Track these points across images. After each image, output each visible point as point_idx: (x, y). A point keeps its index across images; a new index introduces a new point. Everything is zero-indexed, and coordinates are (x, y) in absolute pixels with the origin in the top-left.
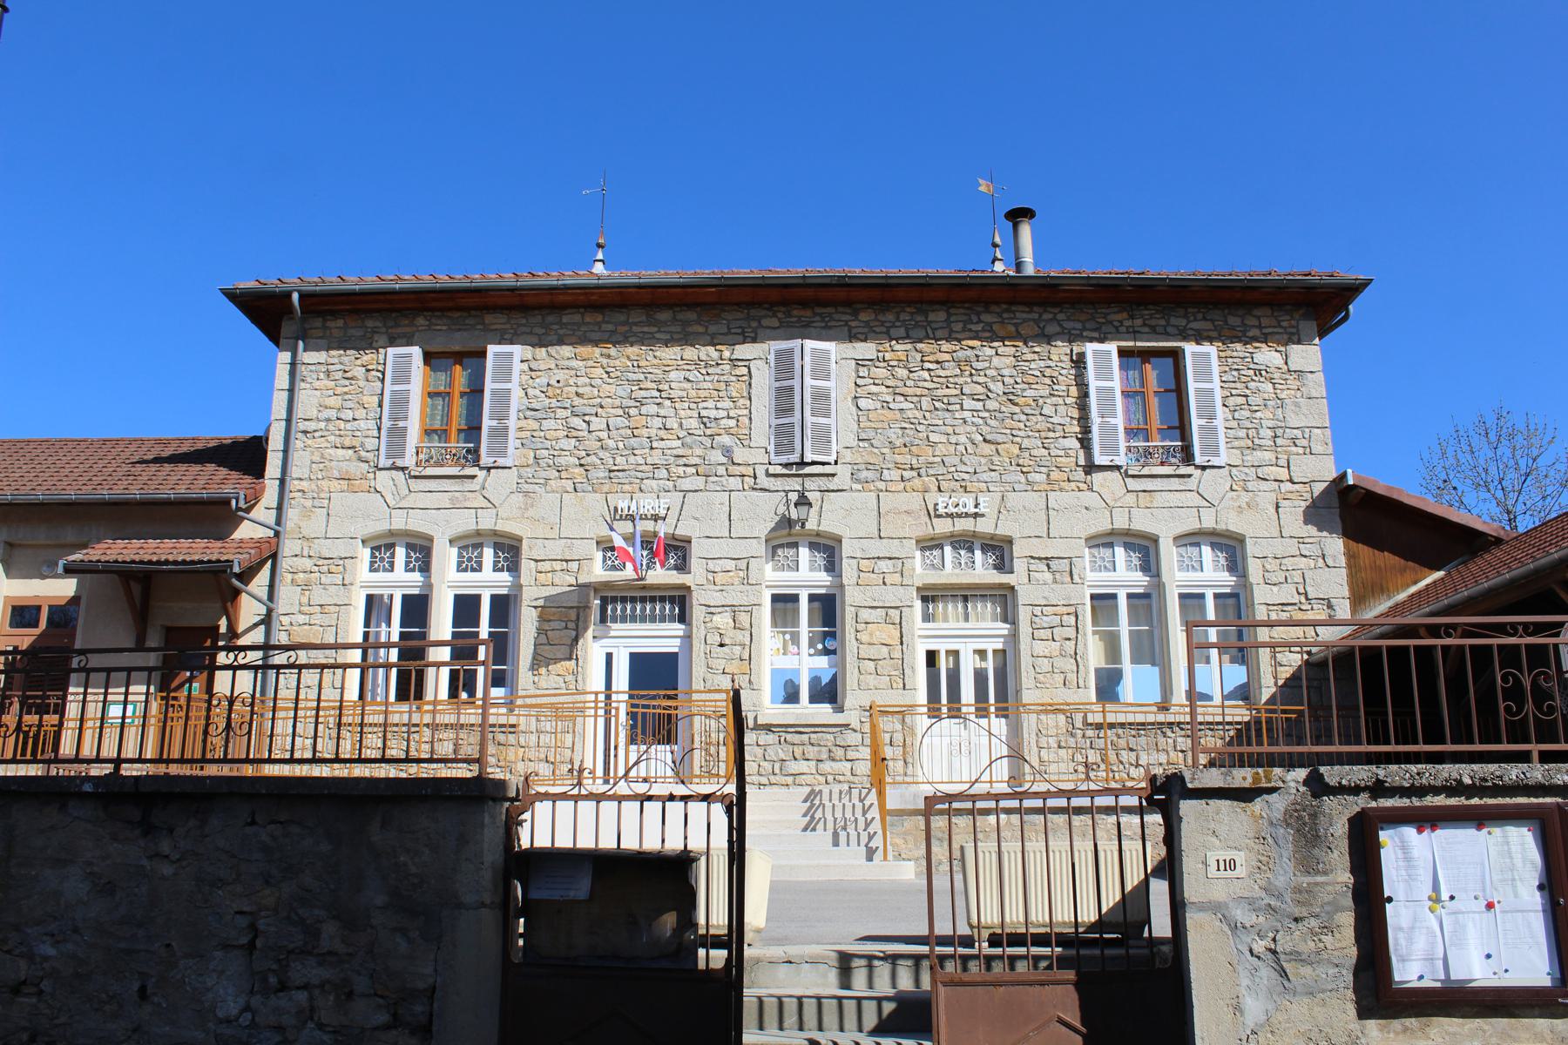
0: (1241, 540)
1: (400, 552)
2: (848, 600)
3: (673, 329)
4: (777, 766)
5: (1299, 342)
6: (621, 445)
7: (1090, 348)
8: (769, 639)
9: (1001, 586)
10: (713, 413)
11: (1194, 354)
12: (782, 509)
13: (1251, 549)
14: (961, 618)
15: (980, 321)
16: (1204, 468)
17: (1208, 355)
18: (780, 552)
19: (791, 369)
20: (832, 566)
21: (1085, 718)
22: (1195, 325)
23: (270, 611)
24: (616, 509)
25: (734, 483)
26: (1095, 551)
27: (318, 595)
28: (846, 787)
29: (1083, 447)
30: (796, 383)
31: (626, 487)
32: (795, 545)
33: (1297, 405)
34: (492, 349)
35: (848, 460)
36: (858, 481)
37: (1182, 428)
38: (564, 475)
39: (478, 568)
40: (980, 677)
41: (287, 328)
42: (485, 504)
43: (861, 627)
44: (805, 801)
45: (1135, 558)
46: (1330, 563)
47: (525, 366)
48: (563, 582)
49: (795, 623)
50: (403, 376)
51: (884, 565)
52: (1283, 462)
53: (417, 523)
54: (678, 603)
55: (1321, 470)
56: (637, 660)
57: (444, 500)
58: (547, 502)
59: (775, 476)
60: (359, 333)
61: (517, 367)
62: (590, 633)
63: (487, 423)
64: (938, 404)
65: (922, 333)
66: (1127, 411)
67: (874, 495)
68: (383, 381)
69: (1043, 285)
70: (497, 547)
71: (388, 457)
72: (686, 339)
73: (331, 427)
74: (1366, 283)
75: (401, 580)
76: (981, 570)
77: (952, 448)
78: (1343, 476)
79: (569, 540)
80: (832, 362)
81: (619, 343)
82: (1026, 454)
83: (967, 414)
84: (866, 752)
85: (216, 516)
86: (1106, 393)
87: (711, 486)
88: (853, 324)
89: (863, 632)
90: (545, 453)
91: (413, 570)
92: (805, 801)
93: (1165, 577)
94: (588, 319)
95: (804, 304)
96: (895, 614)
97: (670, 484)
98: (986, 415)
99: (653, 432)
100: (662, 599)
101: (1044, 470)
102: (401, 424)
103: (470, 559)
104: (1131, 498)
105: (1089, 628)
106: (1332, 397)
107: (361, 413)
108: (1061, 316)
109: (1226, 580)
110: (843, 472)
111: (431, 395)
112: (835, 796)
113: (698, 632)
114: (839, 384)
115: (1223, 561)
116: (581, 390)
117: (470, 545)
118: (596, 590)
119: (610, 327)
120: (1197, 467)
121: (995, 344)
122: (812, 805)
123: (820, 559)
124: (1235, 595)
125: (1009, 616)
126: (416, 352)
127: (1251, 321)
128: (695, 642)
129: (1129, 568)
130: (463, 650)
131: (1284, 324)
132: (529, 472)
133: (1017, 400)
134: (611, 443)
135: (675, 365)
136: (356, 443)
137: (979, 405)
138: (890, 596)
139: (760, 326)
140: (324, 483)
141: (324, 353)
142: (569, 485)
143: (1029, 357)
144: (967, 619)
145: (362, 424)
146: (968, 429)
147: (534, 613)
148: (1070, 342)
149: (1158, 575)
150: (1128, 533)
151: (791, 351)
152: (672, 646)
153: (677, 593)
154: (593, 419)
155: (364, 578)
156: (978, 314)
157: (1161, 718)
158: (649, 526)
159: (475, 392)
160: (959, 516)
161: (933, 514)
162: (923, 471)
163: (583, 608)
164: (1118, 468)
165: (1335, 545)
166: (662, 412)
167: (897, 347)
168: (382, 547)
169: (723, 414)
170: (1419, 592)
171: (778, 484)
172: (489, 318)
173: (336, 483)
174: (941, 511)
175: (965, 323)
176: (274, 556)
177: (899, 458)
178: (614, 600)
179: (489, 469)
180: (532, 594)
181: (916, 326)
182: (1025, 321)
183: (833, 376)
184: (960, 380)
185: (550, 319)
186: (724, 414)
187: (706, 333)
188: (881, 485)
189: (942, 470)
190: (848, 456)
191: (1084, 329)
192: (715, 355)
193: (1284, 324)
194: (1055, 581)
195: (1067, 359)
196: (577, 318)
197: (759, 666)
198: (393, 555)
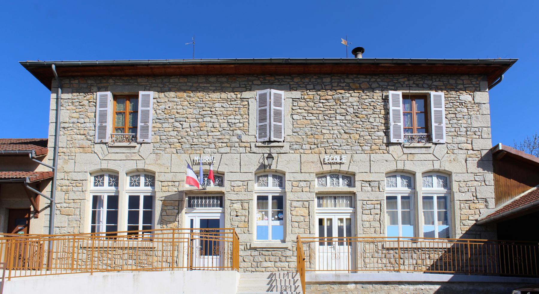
0: (449, 174)
1: (106, 178)
2: (288, 198)
3: (217, 85)
5: (480, 91)
6: (195, 134)
7: (391, 93)
8: (256, 213)
9: (350, 193)
10: (233, 121)
11: (434, 96)
12: (261, 161)
13: (454, 177)
14: (333, 205)
15: (344, 82)
16: (436, 144)
17: (440, 96)
18: (261, 179)
19: (265, 102)
20: (281, 184)
21: (383, 245)
22: (435, 83)
23: (51, 203)
24: (194, 160)
25: (242, 150)
26: (389, 179)
27: (72, 196)
28: (286, 272)
29: (386, 135)
30: (267, 108)
31: (198, 152)
32: (267, 176)
33: (477, 118)
34: (141, 93)
36: (292, 149)
37: (427, 127)
38: (172, 146)
39: (138, 185)
40: (340, 229)
41: (54, 83)
43: (293, 209)
44: (268, 278)
45: (405, 182)
46: (487, 183)
47: (155, 101)
48: (173, 190)
49: (267, 207)
50: (104, 104)
51: (302, 184)
52: (469, 142)
53: (112, 166)
54: (219, 199)
55: (486, 145)
56: (202, 221)
57: (123, 157)
58: (165, 157)
60: (85, 86)
61: (152, 101)
62: (184, 211)
63: (140, 124)
64: (326, 117)
65: (320, 87)
66: (404, 121)
67: (299, 155)
68: (96, 106)
69: (373, 64)
70: (146, 176)
71: (99, 138)
72: (222, 90)
73: (75, 126)
75: (106, 190)
76: (342, 186)
78: (498, 146)
79: (176, 173)
80: (284, 100)
81: (194, 91)
83: (338, 122)
84: (295, 259)
85: (25, 162)
86: (396, 112)
88: (291, 83)
90: (164, 137)
91: (112, 186)
92: (268, 278)
93: (418, 189)
94: (181, 81)
95: (271, 74)
96: (306, 204)
98: (346, 122)
99: (209, 129)
100: (213, 198)
101: (369, 145)
102: (104, 124)
103: (135, 181)
104: (405, 157)
105: (386, 210)
106: (492, 114)
107: (87, 120)
108: (378, 80)
109: (442, 191)
110: (286, 145)
111: (118, 113)
112: (282, 276)
113: (228, 211)
114: (285, 108)
115: (441, 183)
116: (178, 111)
117: (135, 175)
118: (186, 194)
119: (190, 84)
120: (433, 143)
121: (351, 92)
122: (271, 280)
123: (277, 182)
124: (445, 198)
126: (109, 94)
127: (460, 82)
128: (226, 215)
129: (402, 186)
130: (133, 217)
131: (474, 83)
132: (157, 145)
133: (359, 115)
134: (191, 133)
135: (218, 101)
136: (86, 132)
137: (343, 118)
138: (305, 196)
139: (253, 84)
140: (73, 149)
141: (70, 94)
143: (365, 97)
144: (335, 206)
145: (88, 125)
146: (338, 128)
147: (161, 203)
148: (382, 91)
149: (414, 188)
150: (403, 171)
151: (266, 94)
152: (217, 216)
154: (184, 123)
155: (91, 188)
156: (344, 79)
157: (414, 245)
158: (207, 167)
159: (135, 112)
160: (334, 164)
161: (323, 163)
162: (319, 145)
163: (181, 201)
164: (400, 144)
165: (490, 176)
166: (212, 120)
167: (310, 93)
168: (99, 176)
169: (238, 121)
170: (525, 196)
172: (140, 80)
173: (78, 149)
174: (326, 161)
175: (338, 83)
176: (52, 179)
177: (309, 140)
178: (194, 198)
179: (141, 144)
181: (317, 84)
182: (363, 82)
183: (283, 105)
184: (336, 107)
185: (165, 80)
186: (238, 121)
187: (230, 87)
188: (302, 151)
189: (327, 145)
190: (288, 139)
191: (388, 85)
192: (234, 96)
193: (474, 83)
194: (372, 191)
195: (380, 98)
196: (176, 80)
197: (252, 224)
198: (103, 179)
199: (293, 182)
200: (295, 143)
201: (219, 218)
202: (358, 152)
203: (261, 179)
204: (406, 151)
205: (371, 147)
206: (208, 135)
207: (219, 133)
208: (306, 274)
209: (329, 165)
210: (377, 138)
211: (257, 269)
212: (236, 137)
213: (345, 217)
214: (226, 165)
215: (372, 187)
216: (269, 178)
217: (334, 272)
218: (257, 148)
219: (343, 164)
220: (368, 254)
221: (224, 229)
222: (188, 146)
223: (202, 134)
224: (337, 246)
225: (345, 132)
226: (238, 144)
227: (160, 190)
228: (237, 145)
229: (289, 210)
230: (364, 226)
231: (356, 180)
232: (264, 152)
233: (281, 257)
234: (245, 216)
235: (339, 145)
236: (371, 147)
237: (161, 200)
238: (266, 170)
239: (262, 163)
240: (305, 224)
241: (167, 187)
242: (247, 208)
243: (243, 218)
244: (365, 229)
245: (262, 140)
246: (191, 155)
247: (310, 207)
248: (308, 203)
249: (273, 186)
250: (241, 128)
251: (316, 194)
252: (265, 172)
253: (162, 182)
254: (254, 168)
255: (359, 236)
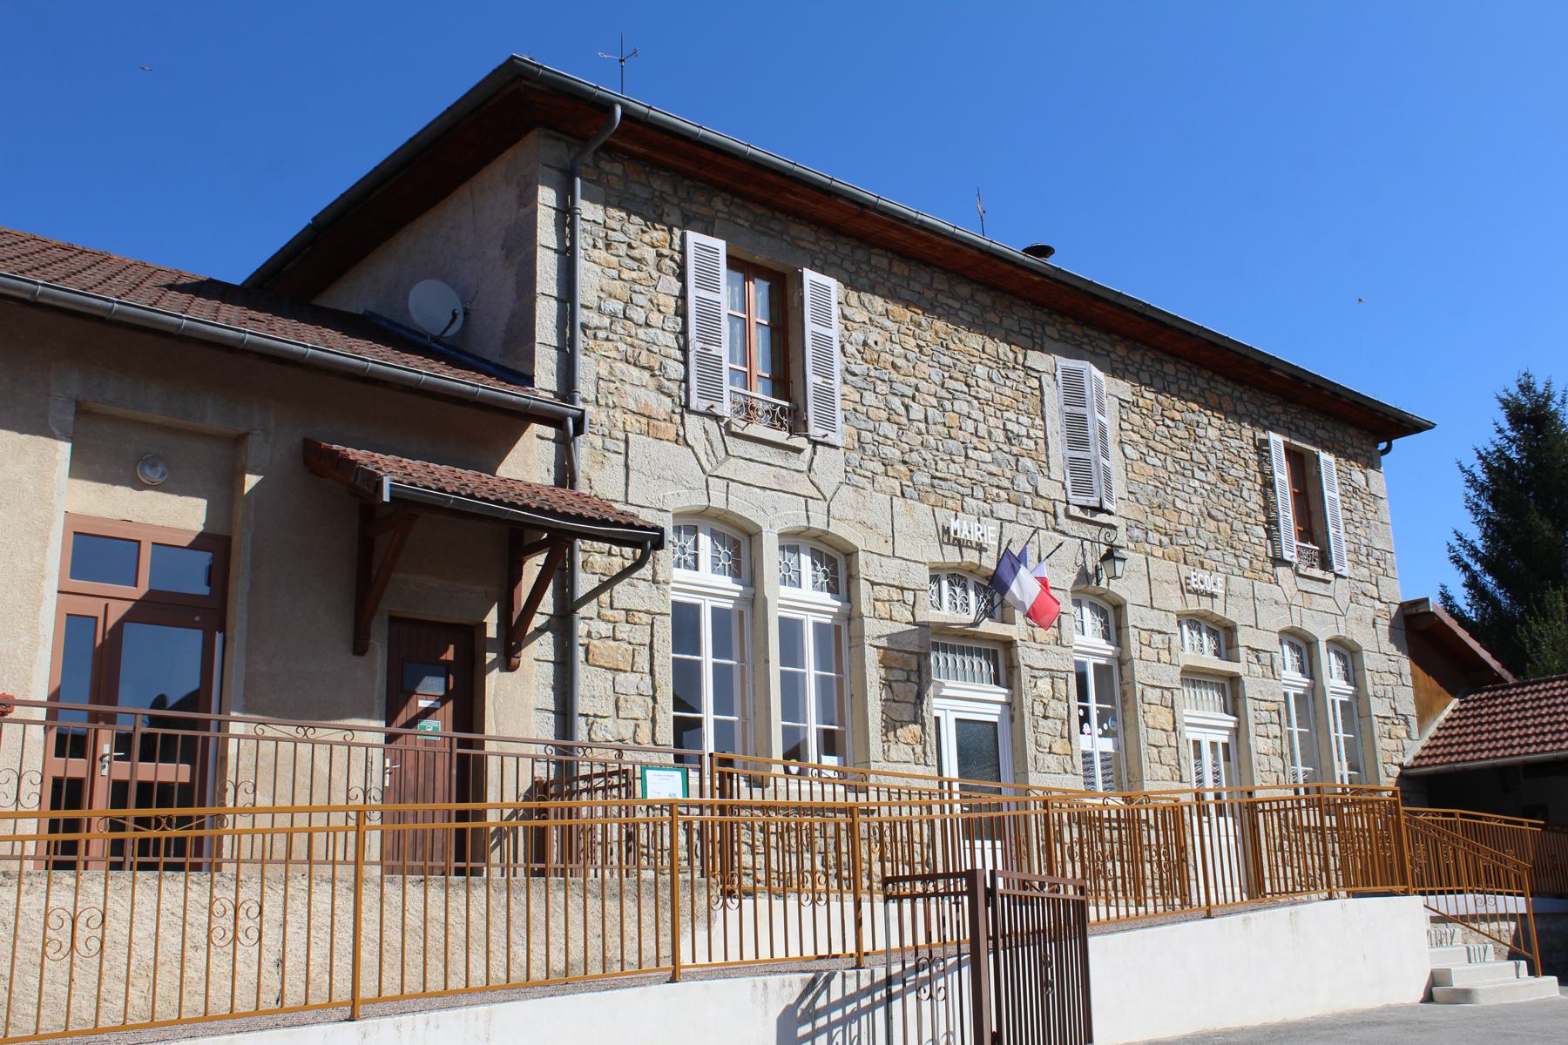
31: (950, 503)
42: (815, 494)
60: (645, 194)
72: (986, 329)
74: (1428, 426)
96: (1167, 694)
172: (796, 229)
180: (875, 629)
201: (995, 719)
204: (1305, 585)
213: (1222, 738)
245: (1082, 500)
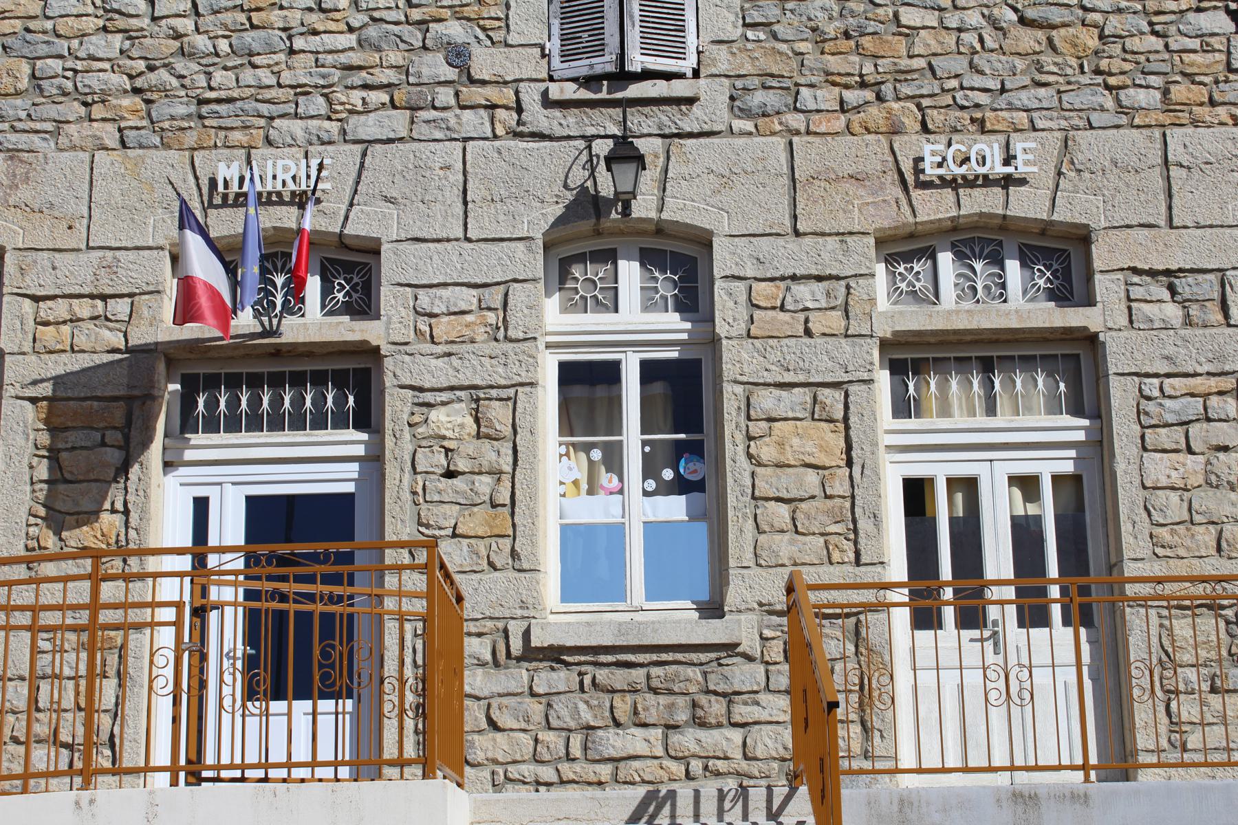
2: (729, 369)
4: (576, 742)
6: (223, 45)
8: (554, 462)
12: (579, 176)
14: (979, 405)
18: (577, 271)
20: (693, 298)
24: (213, 183)
25: (473, 122)
28: (731, 784)
31: (237, 137)
32: (610, 256)
35: (723, 67)
36: (746, 113)
38: (98, 111)
40: (1026, 535)
43: (757, 428)
48: (100, 343)
49: (614, 423)
51: (805, 293)
54: (350, 384)
59: (564, 104)
67: (780, 142)
76: (1021, 300)
77: (950, 40)
82: (1116, 49)
84: (779, 707)
87: (422, 131)
89: (765, 443)
90: (56, 65)
96: (833, 398)
97: (334, 127)
99: (295, 17)
100: (319, 379)
101: (1154, 80)
110: (713, 100)
113: (398, 447)
118: (170, 362)
125: (1086, 397)
128: (391, 470)
134: (202, 42)
138: (821, 361)
142: (109, 134)
144: (991, 410)
152: (340, 479)
153: (349, 365)
158: (286, 217)
160: (970, 183)
161: (914, 180)
162: (887, 89)
171: (571, 122)
174: (931, 172)
178: (212, 383)
188: (796, 121)
189: (929, 86)
190: (722, 60)
194: (1188, 322)
197: (533, 515)
199: (755, 285)
200: (756, 81)
201: (349, 488)
202: (1096, 118)
203: (577, 271)
205: (1166, 92)
206: (292, 52)
207: (351, 40)
208: (845, 793)
209: (948, 193)
210: (1195, 44)
211: (567, 770)
212: (440, 57)
213: (1047, 467)
214: (387, 199)
215: (1184, 303)
216: (622, 264)
217: (1003, 779)
218: (557, 113)
219: (1022, 182)
220: (1191, 674)
221: (380, 546)
222: (181, 110)
223: (256, 47)
224: (1014, 634)
225: (1023, 21)
226: (450, 91)
227: (27, 347)
228: (445, 96)
229: (740, 437)
230: (1156, 517)
231: (1098, 264)
232: (591, 131)
233: (703, 699)
234: (497, 473)
235: (994, 84)
236: (1166, 92)
237: (33, 400)
238: (605, 224)
239: (583, 189)
240: (828, 512)
241: (66, 329)
242: (507, 431)
243: (484, 484)
244: (1163, 533)
245: (581, 67)
246: (199, 157)
247: (853, 420)
248: (839, 395)
249: (646, 308)
250: (467, 11)
251: (884, 345)
252: (598, 233)
253: (36, 299)
254: (539, 218)
255: (1130, 569)
